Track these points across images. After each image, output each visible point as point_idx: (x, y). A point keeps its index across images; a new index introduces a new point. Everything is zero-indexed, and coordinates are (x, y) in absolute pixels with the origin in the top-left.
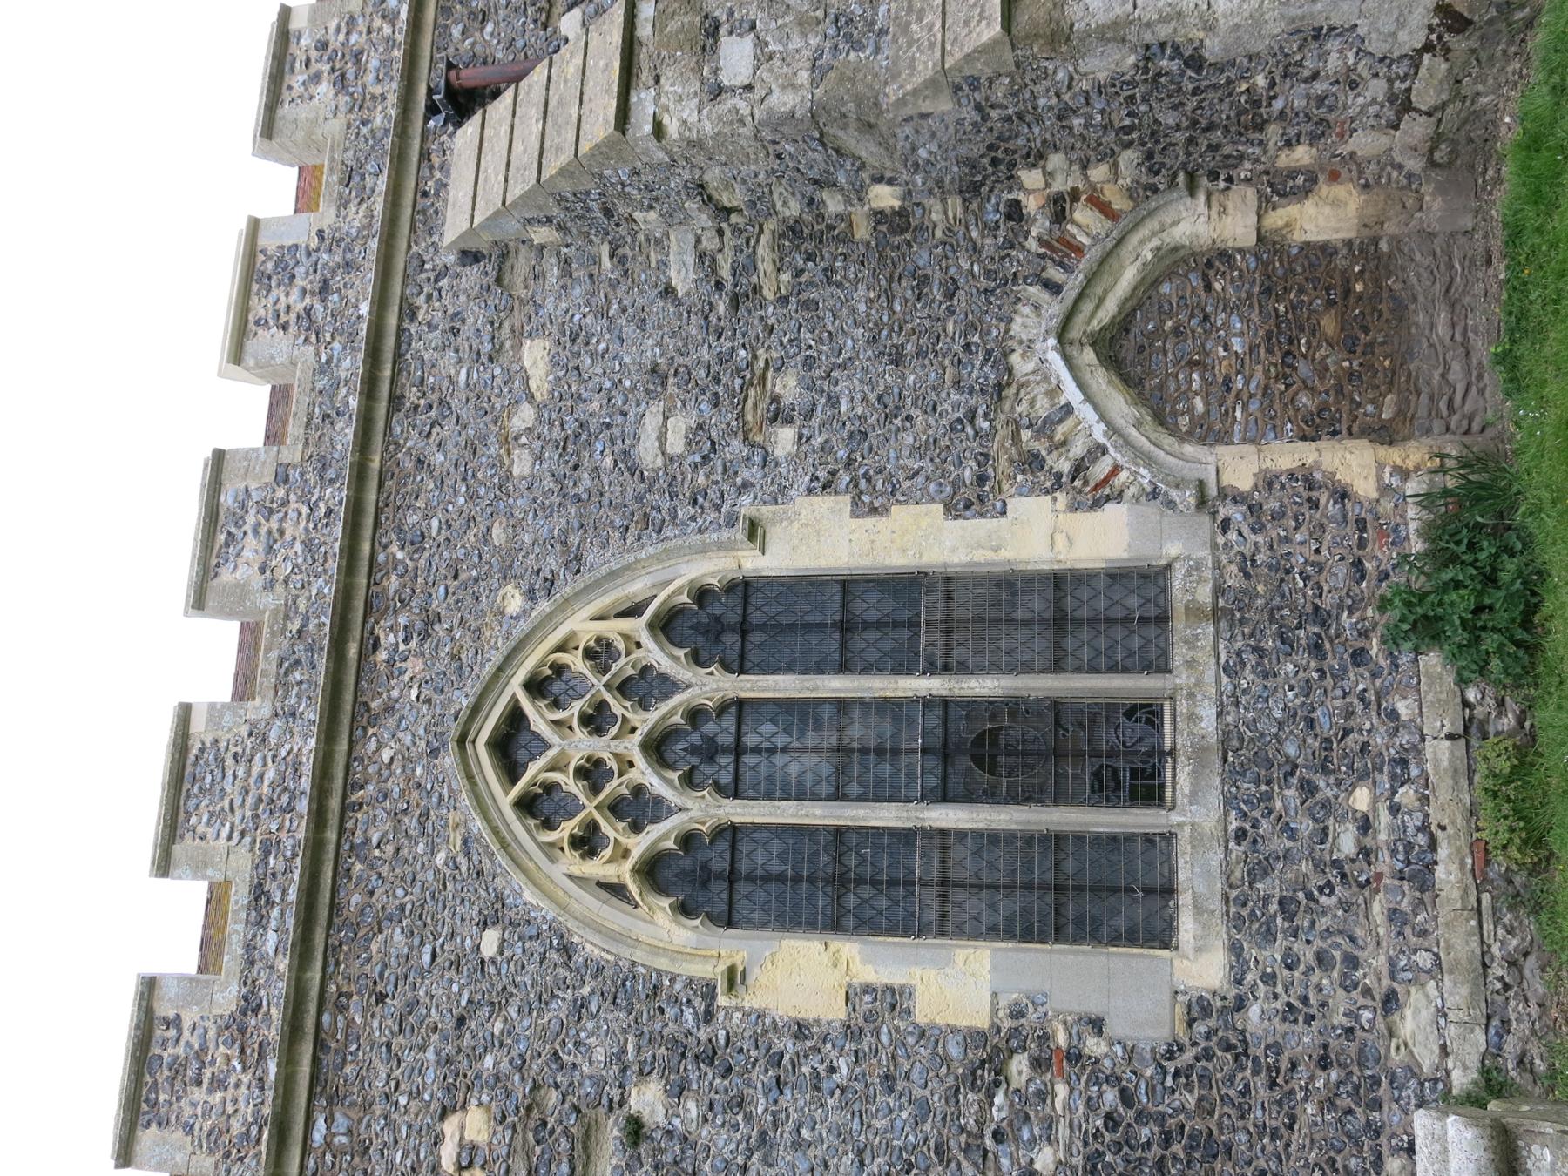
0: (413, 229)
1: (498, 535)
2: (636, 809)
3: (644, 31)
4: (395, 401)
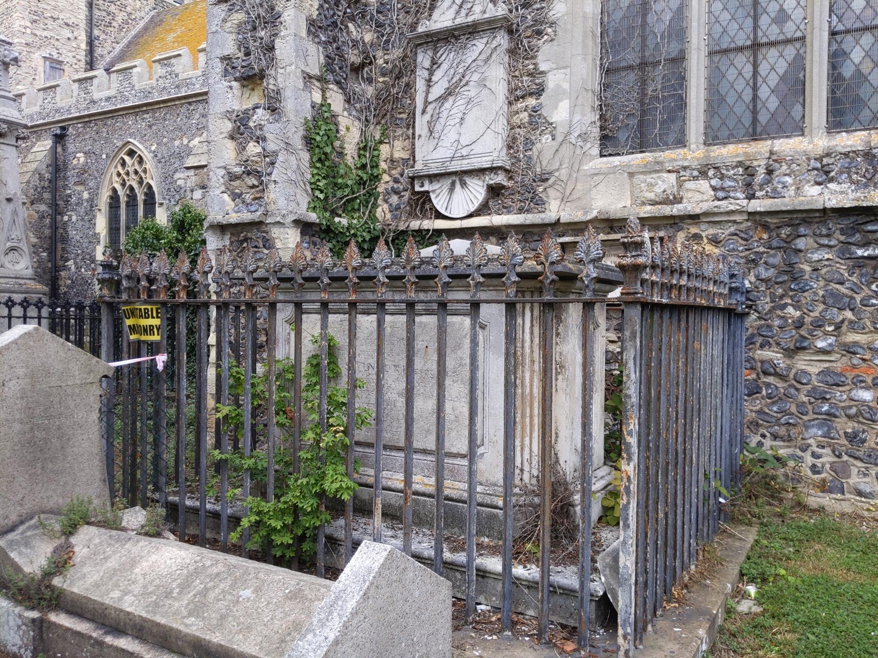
1: (165, 140)
4: (190, 104)
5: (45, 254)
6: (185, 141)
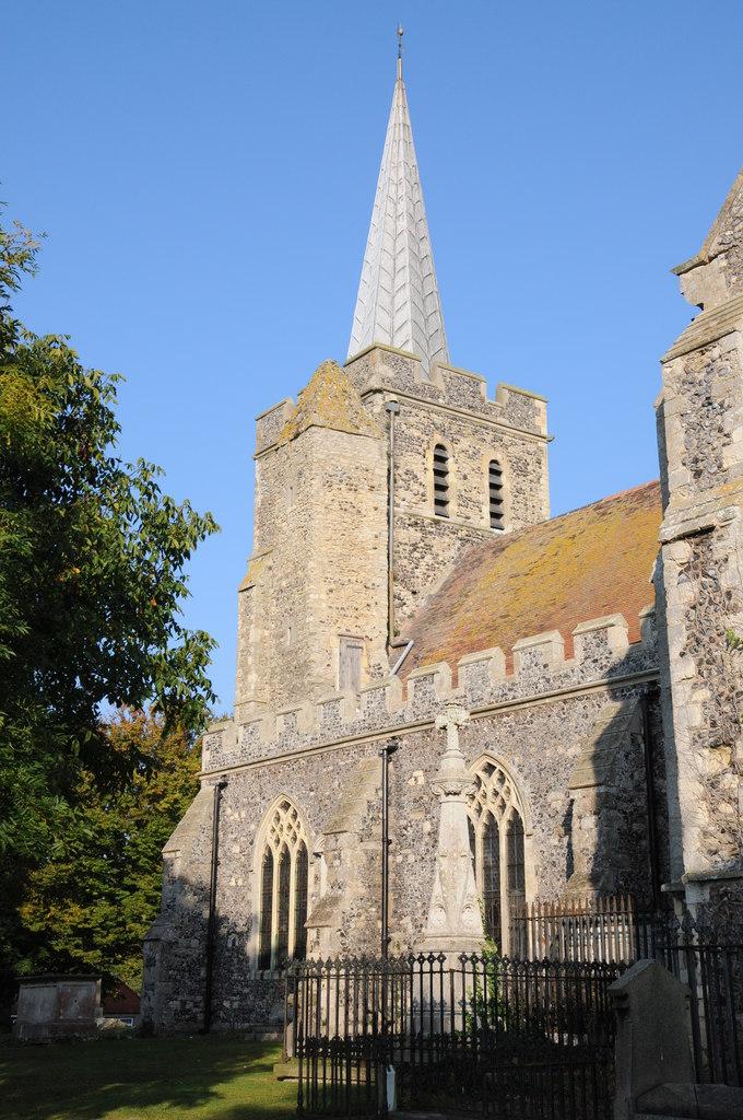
1: (533, 749)
5: (374, 910)
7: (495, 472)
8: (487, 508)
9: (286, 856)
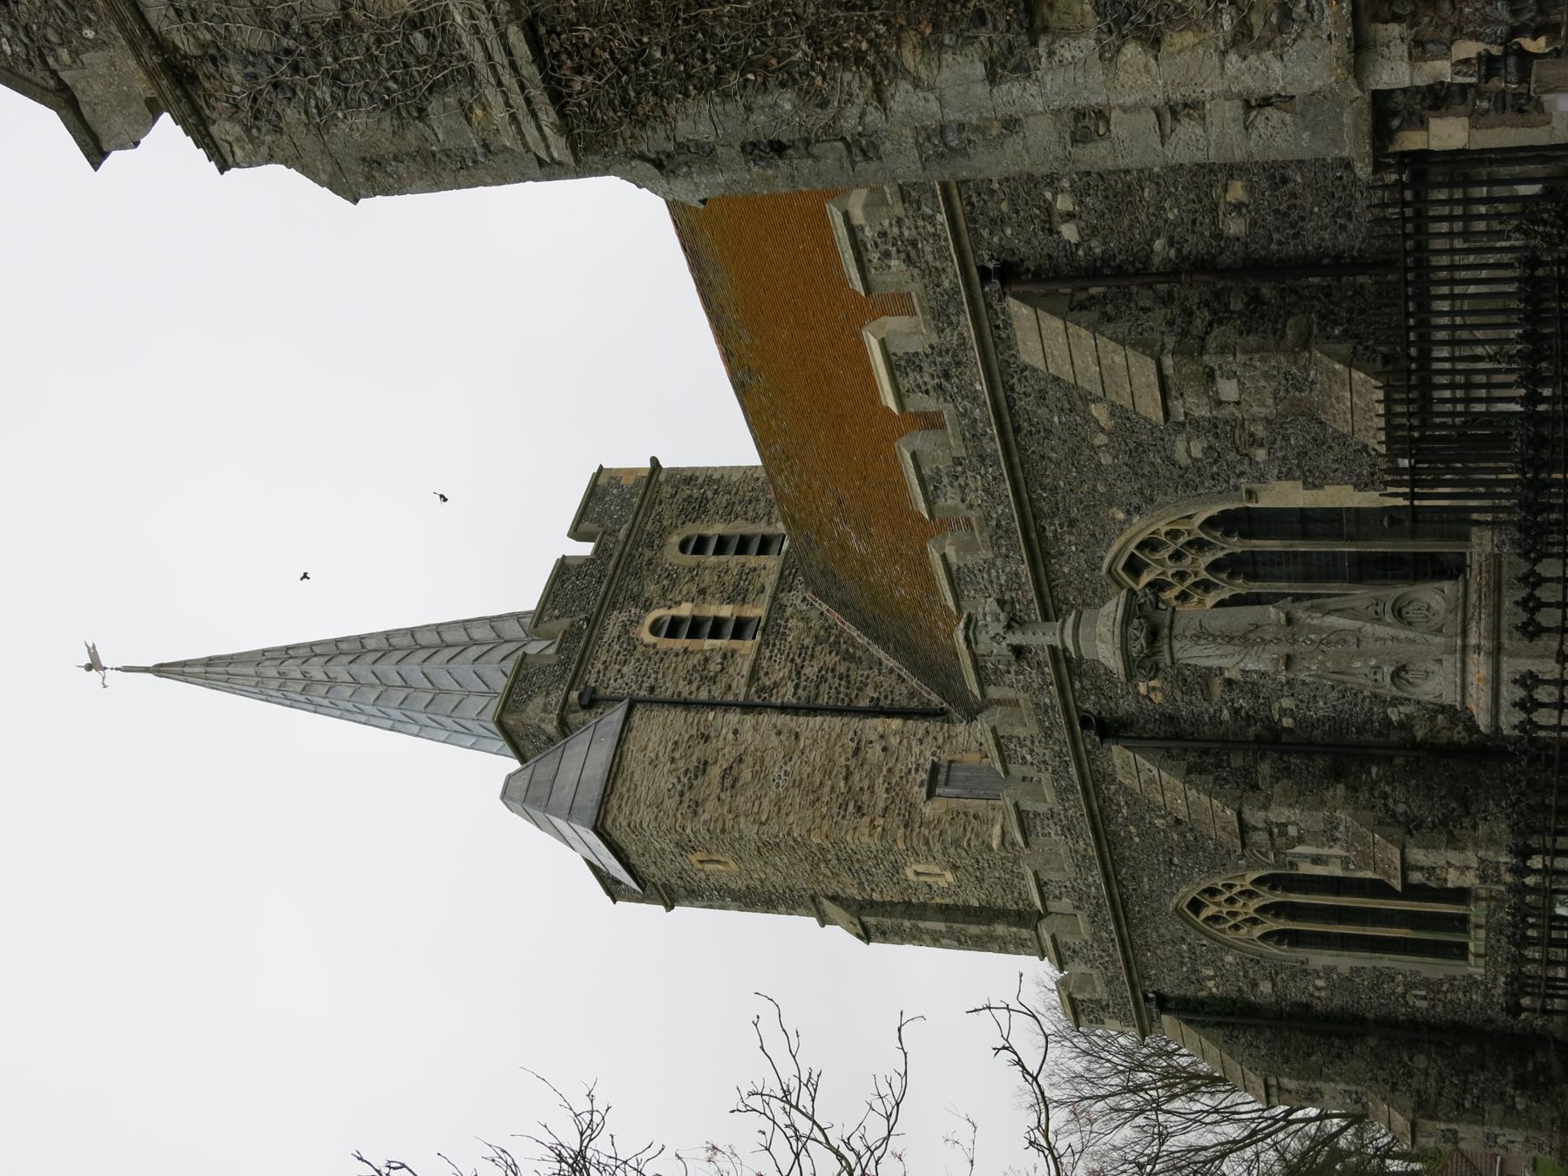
0: (996, 346)
1: (1101, 488)
2: (1206, 586)
3: (1169, 371)
4: (1017, 430)
5: (1374, 770)
6: (1100, 439)
7: (700, 545)
8: (752, 560)
9: (1277, 910)
